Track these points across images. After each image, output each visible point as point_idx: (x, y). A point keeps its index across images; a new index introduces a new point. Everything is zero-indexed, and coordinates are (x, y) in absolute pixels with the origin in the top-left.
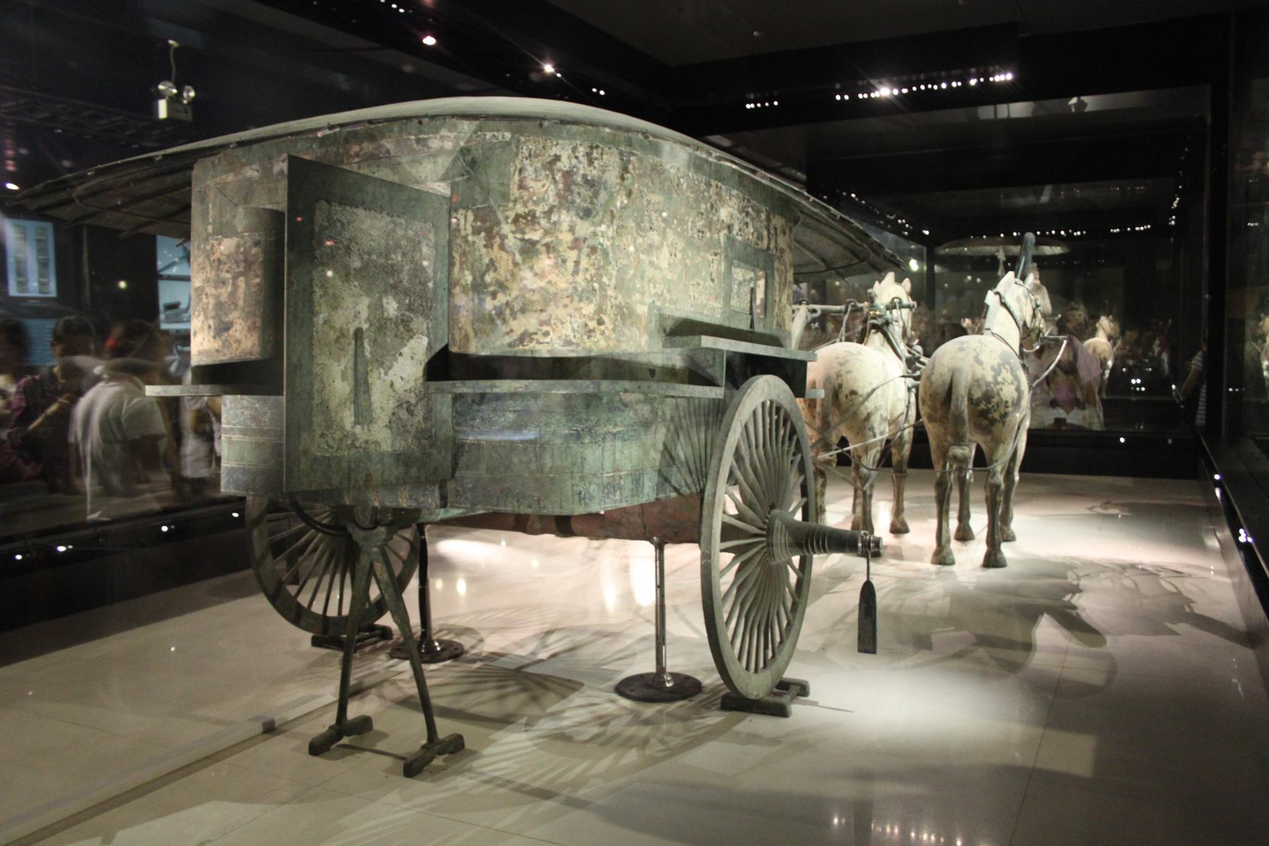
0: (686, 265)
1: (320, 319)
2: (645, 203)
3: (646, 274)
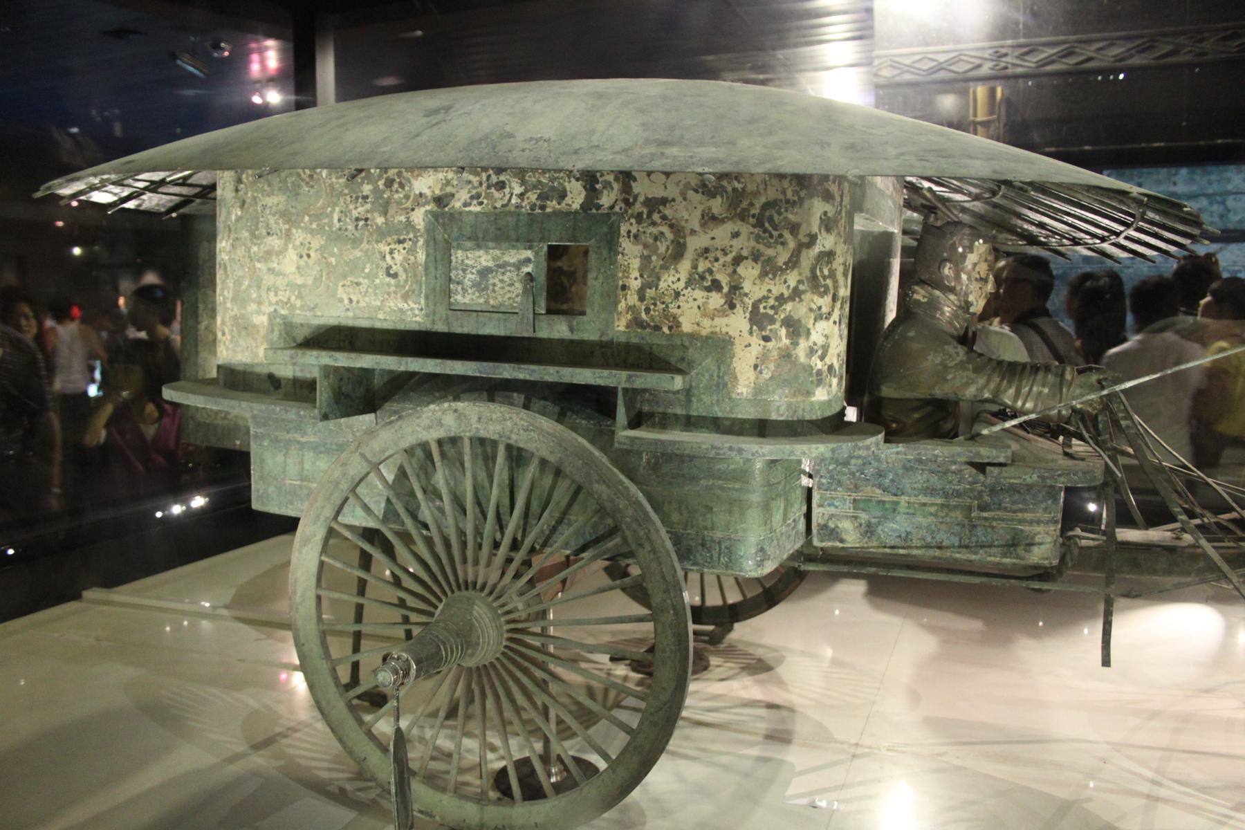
0: (329, 264)
1: (202, 326)
2: (259, 209)
3: (264, 282)
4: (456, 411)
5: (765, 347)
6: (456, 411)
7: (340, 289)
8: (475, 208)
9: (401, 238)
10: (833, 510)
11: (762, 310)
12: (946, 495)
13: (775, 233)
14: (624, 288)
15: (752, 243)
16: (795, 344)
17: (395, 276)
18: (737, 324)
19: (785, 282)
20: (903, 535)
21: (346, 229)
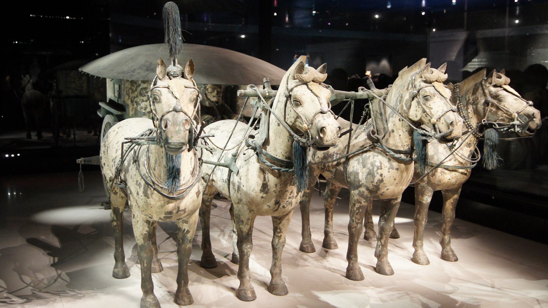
16: (137, 107)
18: (129, 102)
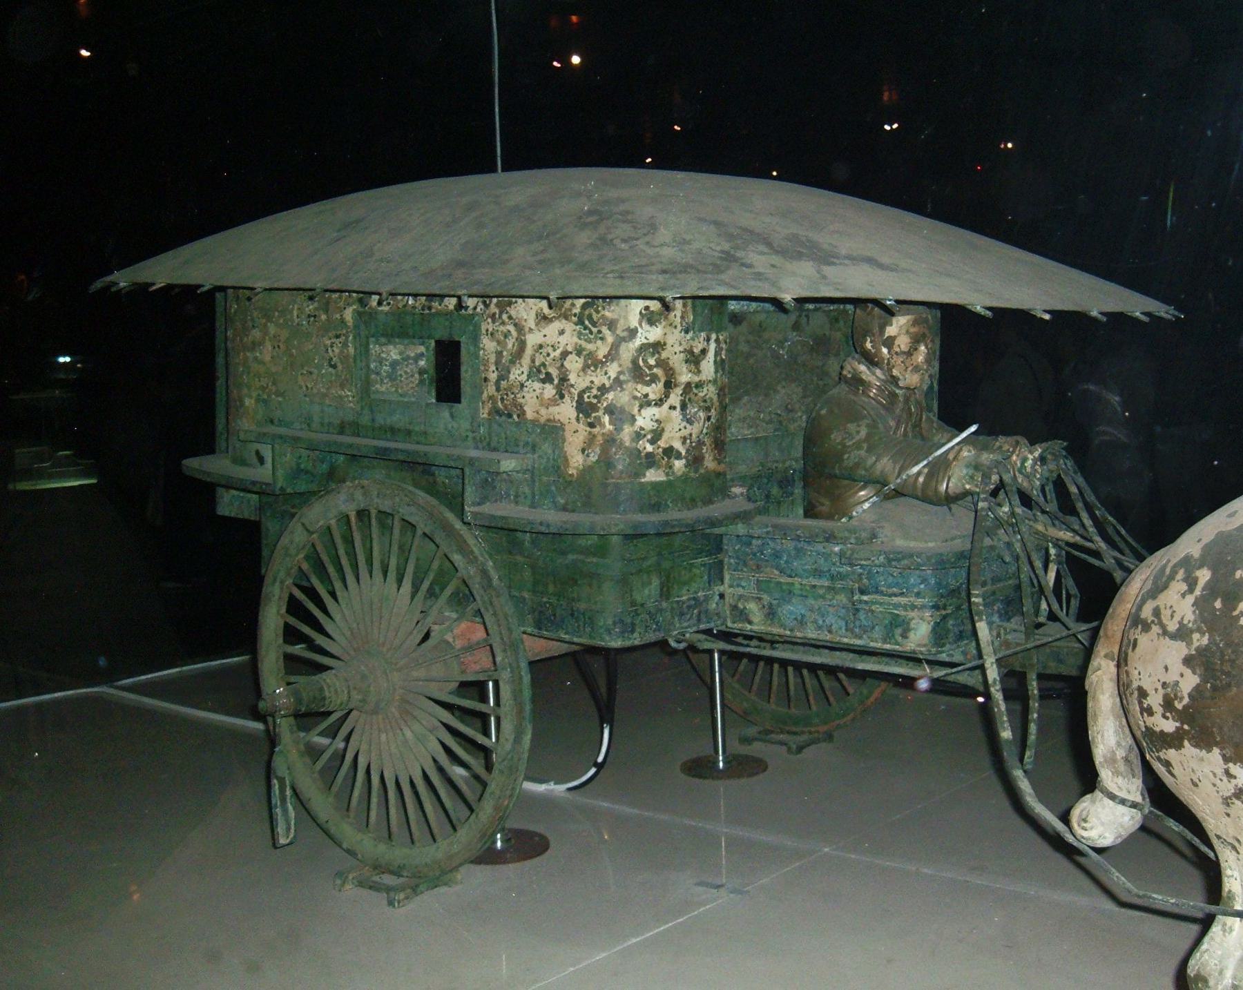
4: (363, 487)
5: (590, 432)
6: (363, 487)
7: (300, 377)
8: (385, 308)
9: (338, 333)
10: (740, 591)
11: (586, 400)
12: (832, 578)
13: (595, 330)
14: (486, 380)
15: (575, 339)
16: (619, 430)
17: (334, 367)
19: (606, 374)
20: (799, 618)
21: (302, 325)
